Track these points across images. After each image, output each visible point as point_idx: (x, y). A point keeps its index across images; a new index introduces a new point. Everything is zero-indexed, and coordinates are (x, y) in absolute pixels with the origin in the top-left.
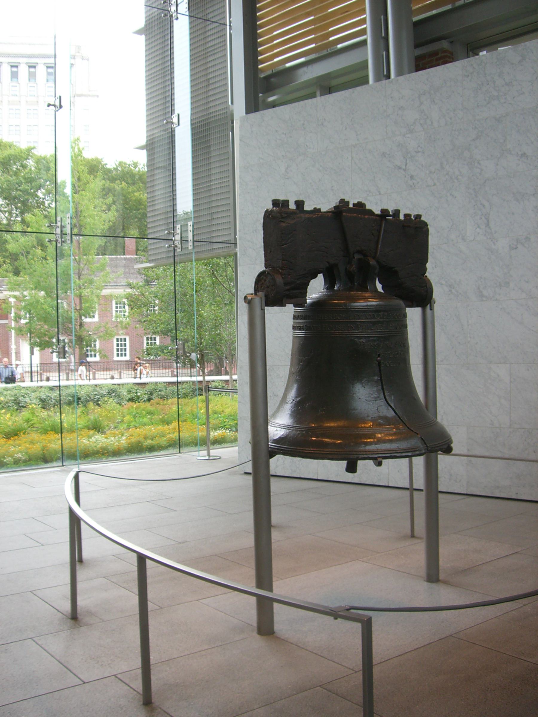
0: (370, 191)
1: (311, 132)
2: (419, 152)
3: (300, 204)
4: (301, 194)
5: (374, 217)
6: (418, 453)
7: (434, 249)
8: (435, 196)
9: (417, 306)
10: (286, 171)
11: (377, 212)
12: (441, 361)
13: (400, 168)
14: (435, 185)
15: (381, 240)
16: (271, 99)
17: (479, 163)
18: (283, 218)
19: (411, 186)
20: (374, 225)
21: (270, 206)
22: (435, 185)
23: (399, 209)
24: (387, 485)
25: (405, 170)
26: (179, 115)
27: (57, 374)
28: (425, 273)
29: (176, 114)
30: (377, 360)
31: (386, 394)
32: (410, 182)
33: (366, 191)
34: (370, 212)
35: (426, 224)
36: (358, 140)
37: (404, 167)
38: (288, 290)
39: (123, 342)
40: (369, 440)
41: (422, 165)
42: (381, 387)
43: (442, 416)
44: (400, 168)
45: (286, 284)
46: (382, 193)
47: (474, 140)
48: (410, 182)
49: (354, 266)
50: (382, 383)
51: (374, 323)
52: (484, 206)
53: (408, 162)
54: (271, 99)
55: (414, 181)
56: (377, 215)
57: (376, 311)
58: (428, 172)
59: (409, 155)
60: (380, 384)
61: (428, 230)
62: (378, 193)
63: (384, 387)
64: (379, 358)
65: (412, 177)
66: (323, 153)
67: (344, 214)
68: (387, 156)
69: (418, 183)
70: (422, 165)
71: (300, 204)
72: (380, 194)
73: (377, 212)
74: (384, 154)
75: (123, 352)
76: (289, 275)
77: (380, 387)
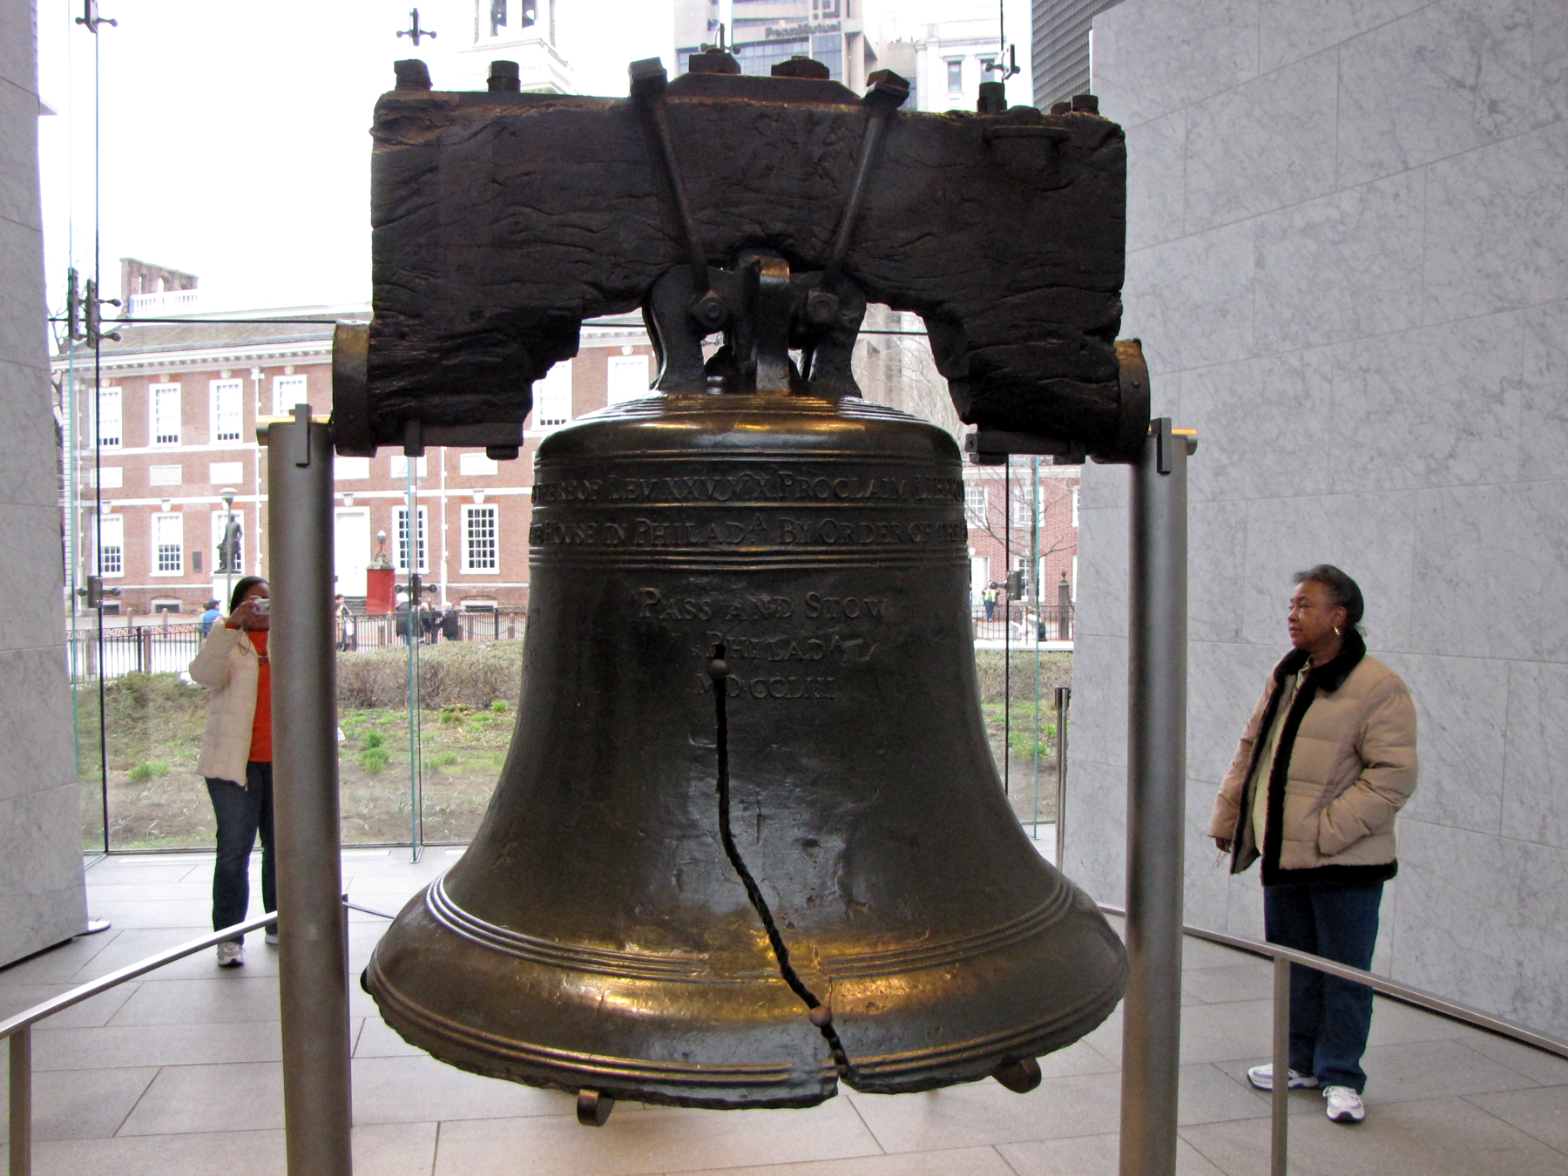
0: (1381, 164)
1: (1246, 26)
4: (1218, 193)
6: (782, 1093)
7: (1545, 313)
8: (1558, 155)
9: (1104, 456)
10: (1187, 137)
12: (1551, 653)
13: (1461, 84)
14: (1558, 117)
19: (1490, 133)
20: (833, 137)
25: (1473, 89)
26: (1012, 48)
27: (1003, 625)
28: (1115, 326)
31: (735, 811)
32: (1488, 123)
33: (1372, 165)
34: (844, 94)
36: (1356, 25)
37: (1470, 81)
41: (1523, 66)
42: (715, 782)
43: (1544, 818)
44: (1461, 84)
45: (377, 371)
46: (1411, 165)
48: (1488, 123)
49: (711, 294)
50: (723, 763)
51: (703, 517)
53: (1484, 62)
55: (1499, 118)
57: (714, 467)
58: (1538, 83)
59: (1488, 42)
60: (716, 771)
61: (1122, 155)
62: (1401, 167)
63: (732, 783)
64: (720, 664)
65: (1493, 107)
66: (1272, 76)
68: (1428, 55)
69: (1510, 120)
70: (1523, 66)
71: (504, 75)
72: (1407, 169)
74: (1420, 53)
76: (403, 336)
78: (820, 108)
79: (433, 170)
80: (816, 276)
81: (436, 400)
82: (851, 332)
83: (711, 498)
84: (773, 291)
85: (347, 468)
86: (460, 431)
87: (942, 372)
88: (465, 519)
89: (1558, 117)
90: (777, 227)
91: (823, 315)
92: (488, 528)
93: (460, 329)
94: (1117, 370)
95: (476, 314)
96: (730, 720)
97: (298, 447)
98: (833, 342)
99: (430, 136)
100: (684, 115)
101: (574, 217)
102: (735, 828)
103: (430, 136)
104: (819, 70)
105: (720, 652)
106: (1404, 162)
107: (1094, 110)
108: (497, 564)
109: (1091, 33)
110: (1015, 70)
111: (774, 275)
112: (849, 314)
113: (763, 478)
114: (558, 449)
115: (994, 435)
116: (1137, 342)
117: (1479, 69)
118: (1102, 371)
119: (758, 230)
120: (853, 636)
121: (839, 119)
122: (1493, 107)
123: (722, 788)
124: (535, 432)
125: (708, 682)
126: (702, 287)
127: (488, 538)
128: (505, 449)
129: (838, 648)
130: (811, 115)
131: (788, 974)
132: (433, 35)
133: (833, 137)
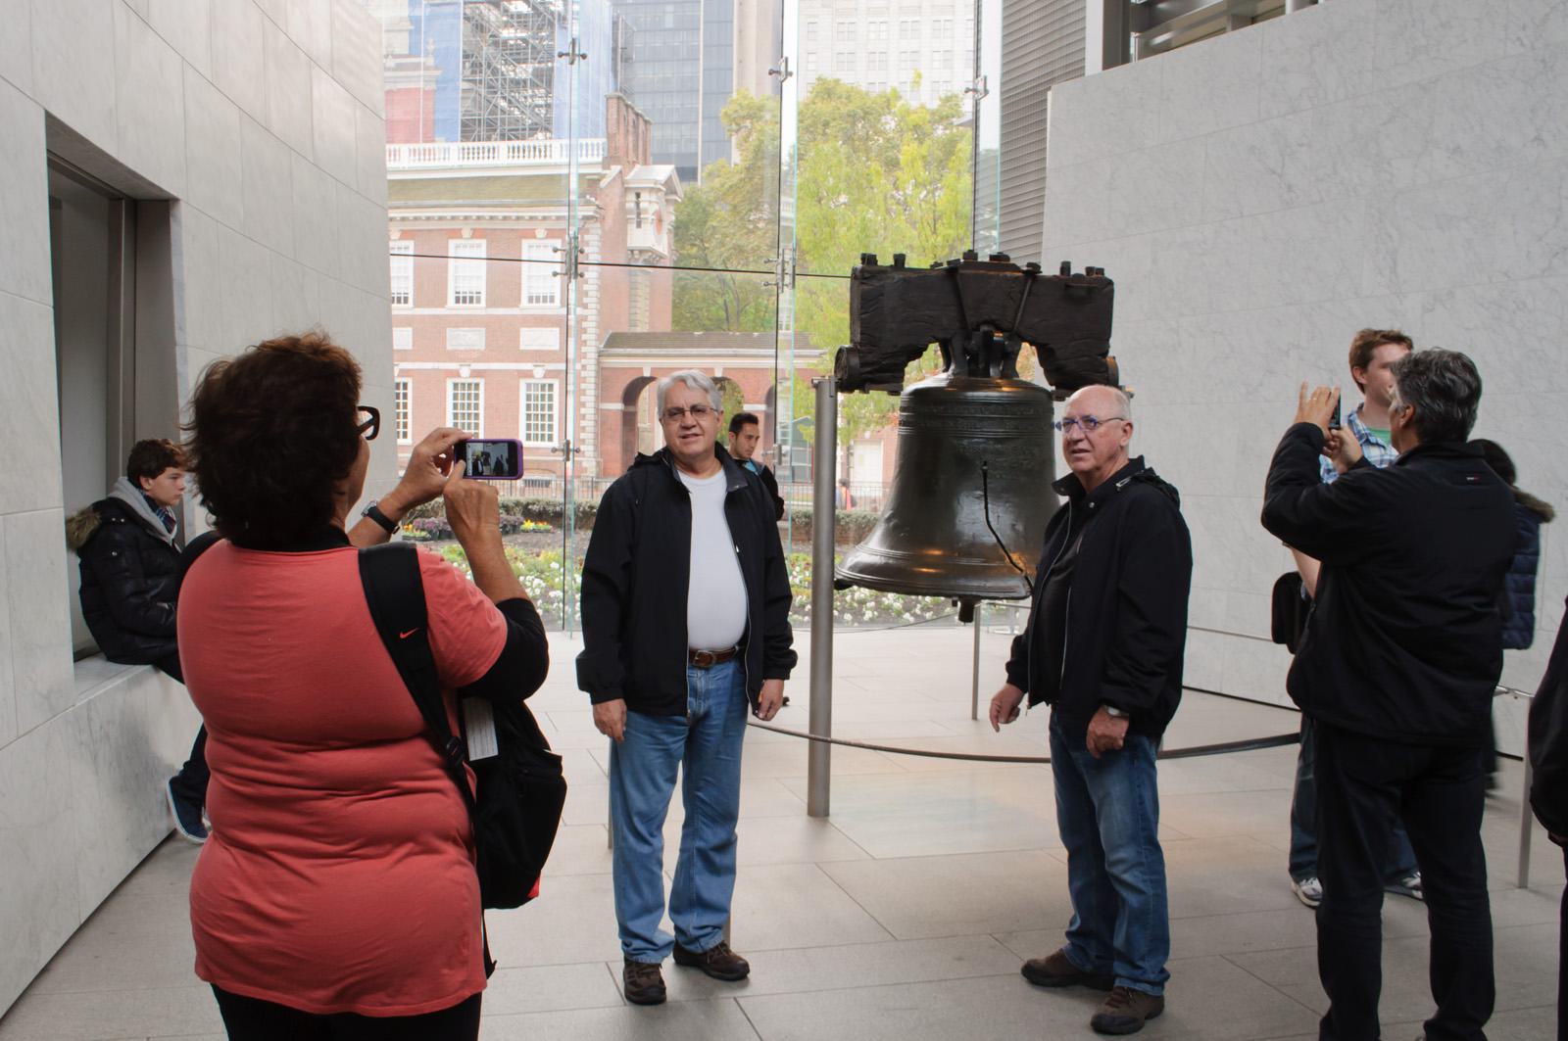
2: (1301, 145)
3: (900, 259)
5: (1020, 274)
11: (1022, 264)
13: (1274, 172)
15: (1022, 306)
16: (1159, 40)
17: (1389, 163)
18: (866, 278)
20: (1014, 285)
21: (859, 264)
22: (1322, 201)
23: (1068, 260)
24: (1219, 691)
25: (1280, 176)
26: (985, 78)
28: (1107, 352)
29: (982, 77)
30: (983, 470)
31: (990, 514)
34: (1016, 268)
35: (1110, 283)
38: (870, 372)
39: (473, 421)
40: (925, 570)
44: (1274, 172)
45: (863, 365)
47: (1385, 124)
52: (1390, 237)
54: (1159, 40)
56: (1023, 272)
61: (1112, 291)
63: (989, 506)
64: (985, 468)
65: (1290, 188)
67: (961, 271)
71: (900, 259)
73: (1022, 264)
75: (546, 432)
76: (870, 353)
77: (983, 505)
78: (1008, 274)
79: (882, 295)
80: (1007, 334)
81: (877, 375)
82: (1016, 354)
83: (982, 413)
84: (998, 342)
85: (841, 396)
86: (881, 386)
87: (1042, 365)
88: (450, 391)
89: (1322, 201)
90: (994, 317)
91: (1010, 349)
92: (546, 403)
93: (889, 351)
94: (1107, 368)
95: (895, 346)
96: (988, 486)
97: (828, 389)
98: (1008, 357)
99: (882, 283)
100: (958, 276)
101: (928, 312)
102: (990, 519)
103: (882, 283)
104: (1007, 258)
105: (985, 464)
106: (1241, 213)
107: (1103, 274)
108: (409, 435)
109: (1049, 93)
110: (986, 92)
111: (998, 336)
112: (1016, 348)
113: (1000, 408)
114: (918, 394)
115: (1062, 391)
116: (1114, 358)
117: (1284, 165)
118: (1102, 370)
119: (986, 317)
120: (1025, 460)
121: (1017, 278)
122: (1290, 188)
123: (986, 508)
124: (910, 387)
125: (981, 472)
126: (968, 337)
127: (473, 411)
128: (896, 392)
129: (1022, 464)
130: (1005, 276)
131: (1012, 562)
132: (584, 56)
133: (1014, 285)
